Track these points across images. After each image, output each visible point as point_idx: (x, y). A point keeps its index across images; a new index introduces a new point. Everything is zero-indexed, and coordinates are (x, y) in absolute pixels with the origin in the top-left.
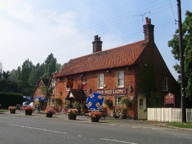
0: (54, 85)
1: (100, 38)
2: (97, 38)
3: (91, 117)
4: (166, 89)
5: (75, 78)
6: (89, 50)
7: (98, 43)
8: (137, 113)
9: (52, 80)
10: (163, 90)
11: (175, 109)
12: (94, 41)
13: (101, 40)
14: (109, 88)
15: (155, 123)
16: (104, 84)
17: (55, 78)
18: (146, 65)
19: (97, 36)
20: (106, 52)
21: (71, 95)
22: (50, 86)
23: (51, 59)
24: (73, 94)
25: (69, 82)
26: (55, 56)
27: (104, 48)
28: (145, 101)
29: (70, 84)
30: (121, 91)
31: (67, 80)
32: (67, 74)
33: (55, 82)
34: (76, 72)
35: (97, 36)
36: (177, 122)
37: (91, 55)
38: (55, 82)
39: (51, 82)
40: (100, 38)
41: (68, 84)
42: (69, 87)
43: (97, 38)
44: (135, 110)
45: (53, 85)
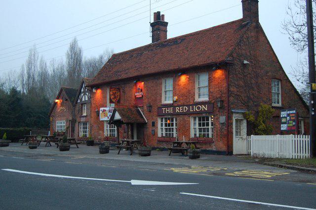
0: (87, 99)
1: (163, 15)
2: (158, 16)
3: (247, 120)
4: (278, 103)
5: (123, 86)
6: (146, 39)
7: (159, 24)
8: (232, 144)
9: (82, 90)
10: (274, 105)
11: (304, 136)
12: (152, 21)
13: (166, 20)
14: (182, 102)
15: (249, 159)
16: (174, 96)
17: (86, 86)
18: (245, 62)
19: (159, 13)
20: (176, 41)
21: (118, 116)
22: (79, 101)
23: (75, 55)
24: (120, 114)
25: (114, 94)
26: (80, 44)
27: (172, 33)
28: (244, 125)
29: (115, 97)
30: (203, 107)
31: (110, 91)
32: (107, 80)
33: (87, 94)
34: (124, 76)
35: (159, 13)
36: (296, 158)
37: (149, 46)
38: (87, 94)
39: (80, 93)
40: (163, 15)
41: (112, 97)
42: (113, 102)
43: (158, 16)
44: (228, 138)
45: (83, 100)
